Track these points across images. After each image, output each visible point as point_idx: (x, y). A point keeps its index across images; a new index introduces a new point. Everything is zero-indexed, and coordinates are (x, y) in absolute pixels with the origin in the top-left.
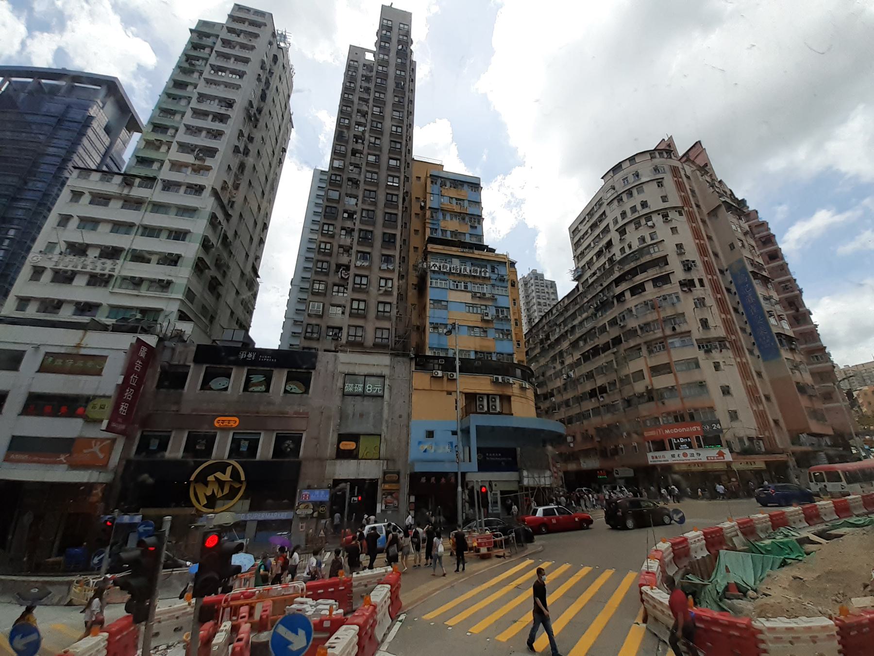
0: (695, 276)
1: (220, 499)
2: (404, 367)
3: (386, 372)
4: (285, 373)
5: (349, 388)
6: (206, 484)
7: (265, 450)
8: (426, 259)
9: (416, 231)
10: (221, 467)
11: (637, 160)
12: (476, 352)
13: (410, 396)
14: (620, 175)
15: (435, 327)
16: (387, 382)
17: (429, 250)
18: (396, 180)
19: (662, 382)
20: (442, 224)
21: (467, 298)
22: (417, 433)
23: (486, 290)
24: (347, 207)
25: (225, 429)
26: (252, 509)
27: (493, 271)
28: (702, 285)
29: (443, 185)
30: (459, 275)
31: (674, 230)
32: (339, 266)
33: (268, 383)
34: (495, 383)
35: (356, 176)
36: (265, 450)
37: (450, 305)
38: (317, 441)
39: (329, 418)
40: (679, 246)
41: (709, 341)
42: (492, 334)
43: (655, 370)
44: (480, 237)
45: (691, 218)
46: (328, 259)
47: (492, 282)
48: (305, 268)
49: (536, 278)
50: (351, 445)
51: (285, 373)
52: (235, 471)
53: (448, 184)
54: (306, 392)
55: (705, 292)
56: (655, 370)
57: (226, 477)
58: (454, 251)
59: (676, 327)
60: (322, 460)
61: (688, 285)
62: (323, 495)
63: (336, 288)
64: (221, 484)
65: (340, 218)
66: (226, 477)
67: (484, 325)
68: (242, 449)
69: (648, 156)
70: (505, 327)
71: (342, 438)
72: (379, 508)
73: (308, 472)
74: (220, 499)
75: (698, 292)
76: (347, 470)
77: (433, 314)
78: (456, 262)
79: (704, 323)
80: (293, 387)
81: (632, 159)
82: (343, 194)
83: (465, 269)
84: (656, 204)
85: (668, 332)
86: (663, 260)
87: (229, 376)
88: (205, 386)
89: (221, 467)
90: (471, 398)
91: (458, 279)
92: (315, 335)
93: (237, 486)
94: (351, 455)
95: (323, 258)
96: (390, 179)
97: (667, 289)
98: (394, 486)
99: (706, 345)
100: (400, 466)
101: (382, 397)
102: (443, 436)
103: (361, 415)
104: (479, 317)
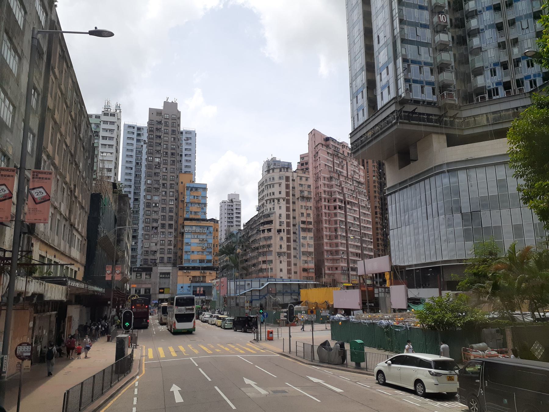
0: (282, 228)
2: (176, 269)
3: (170, 271)
4: (145, 273)
5: (161, 276)
7: (142, 292)
10: (134, 296)
11: (275, 171)
14: (269, 175)
15: (186, 252)
17: (185, 224)
19: (264, 266)
20: (190, 209)
21: (197, 241)
22: (179, 287)
23: (204, 237)
28: (284, 232)
29: (192, 190)
31: (280, 207)
32: (153, 227)
33: (141, 275)
35: (156, 186)
36: (142, 292)
37: (192, 244)
40: (280, 215)
41: (281, 253)
42: (205, 253)
43: (264, 262)
44: (205, 213)
45: (288, 202)
46: (148, 225)
49: (275, 164)
50: (162, 291)
51: (145, 273)
53: (193, 189)
55: (284, 235)
56: (264, 262)
58: (194, 223)
60: (156, 294)
61: (279, 231)
69: (279, 170)
70: (210, 250)
71: (160, 289)
73: (153, 296)
75: (282, 234)
76: (161, 296)
77: (186, 248)
78: (194, 228)
79: (281, 246)
80: (147, 277)
84: (277, 195)
86: (271, 222)
94: (163, 293)
97: (270, 234)
99: (280, 254)
102: (186, 288)
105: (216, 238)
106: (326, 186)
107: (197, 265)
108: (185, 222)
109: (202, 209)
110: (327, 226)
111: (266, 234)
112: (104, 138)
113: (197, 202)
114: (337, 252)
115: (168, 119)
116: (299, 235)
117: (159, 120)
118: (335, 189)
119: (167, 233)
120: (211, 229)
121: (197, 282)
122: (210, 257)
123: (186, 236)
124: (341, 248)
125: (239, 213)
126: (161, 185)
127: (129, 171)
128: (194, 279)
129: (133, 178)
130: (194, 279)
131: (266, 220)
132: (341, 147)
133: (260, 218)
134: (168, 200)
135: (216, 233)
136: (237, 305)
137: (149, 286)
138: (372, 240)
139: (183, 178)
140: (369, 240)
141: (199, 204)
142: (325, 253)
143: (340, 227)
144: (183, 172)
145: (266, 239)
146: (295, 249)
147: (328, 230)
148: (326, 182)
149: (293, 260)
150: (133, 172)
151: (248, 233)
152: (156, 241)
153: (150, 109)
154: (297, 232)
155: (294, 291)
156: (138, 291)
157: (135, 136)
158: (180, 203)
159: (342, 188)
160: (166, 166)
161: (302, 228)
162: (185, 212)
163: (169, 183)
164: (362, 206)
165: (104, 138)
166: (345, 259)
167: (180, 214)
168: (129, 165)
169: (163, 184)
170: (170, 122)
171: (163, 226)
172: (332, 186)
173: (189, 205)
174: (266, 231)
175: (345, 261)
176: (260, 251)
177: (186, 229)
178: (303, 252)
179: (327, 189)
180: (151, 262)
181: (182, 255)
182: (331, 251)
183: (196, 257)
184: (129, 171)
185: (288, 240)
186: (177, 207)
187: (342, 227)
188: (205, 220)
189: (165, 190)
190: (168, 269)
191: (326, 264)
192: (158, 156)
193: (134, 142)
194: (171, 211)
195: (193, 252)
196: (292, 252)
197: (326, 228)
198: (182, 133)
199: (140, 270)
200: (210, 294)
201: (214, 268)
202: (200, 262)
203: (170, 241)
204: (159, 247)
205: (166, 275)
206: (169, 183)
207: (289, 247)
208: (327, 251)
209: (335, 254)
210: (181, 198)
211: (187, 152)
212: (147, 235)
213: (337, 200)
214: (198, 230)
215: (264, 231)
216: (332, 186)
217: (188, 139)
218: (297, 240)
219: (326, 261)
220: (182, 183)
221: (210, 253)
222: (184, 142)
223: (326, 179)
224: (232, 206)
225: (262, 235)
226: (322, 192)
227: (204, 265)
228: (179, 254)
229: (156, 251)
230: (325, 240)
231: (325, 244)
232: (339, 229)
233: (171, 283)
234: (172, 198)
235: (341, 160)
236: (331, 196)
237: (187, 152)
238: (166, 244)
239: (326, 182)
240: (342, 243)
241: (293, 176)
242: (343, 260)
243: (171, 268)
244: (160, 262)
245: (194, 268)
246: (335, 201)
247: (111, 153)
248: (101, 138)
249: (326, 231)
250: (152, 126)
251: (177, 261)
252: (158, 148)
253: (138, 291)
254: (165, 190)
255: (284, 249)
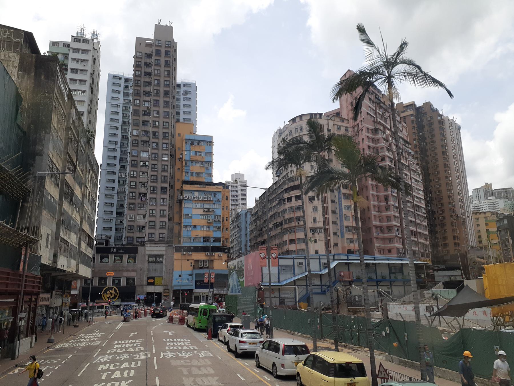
1: (112, 298)
3: (164, 253)
4: (127, 255)
5: (151, 260)
6: (107, 294)
7: (123, 283)
8: (182, 194)
9: (179, 169)
10: (111, 288)
11: (303, 118)
12: (204, 238)
13: (173, 262)
14: (295, 125)
15: (186, 227)
16: (164, 257)
17: (184, 188)
18: (167, 156)
19: (292, 247)
20: (191, 169)
22: (176, 275)
24: (142, 159)
25: (110, 276)
26: (122, 301)
27: (215, 196)
28: (318, 200)
29: (192, 144)
30: (198, 200)
32: (140, 194)
33: (121, 259)
34: (207, 255)
35: (145, 138)
36: (123, 283)
37: (194, 217)
38: (141, 280)
39: (144, 271)
41: (315, 228)
42: (212, 229)
43: (292, 241)
44: (210, 175)
46: (134, 190)
47: (214, 202)
48: (109, 156)
50: (152, 281)
51: (127, 255)
52: (115, 289)
54: (135, 262)
56: (292, 241)
57: (113, 292)
58: (195, 187)
59: (299, 222)
62: (142, 297)
63: (140, 205)
64: (111, 294)
65: (139, 166)
66: (113, 292)
67: (208, 225)
68: (117, 282)
70: (219, 225)
71: (149, 278)
72: (162, 301)
73: (138, 290)
74: (112, 298)
76: (151, 289)
77: (185, 221)
78: (196, 194)
79: (315, 219)
80: (130, 261)
81: (301, 117)
82: (139, 151)
83: (200, 197)
85: (297, 224)
87: (108, 258)
88: (101, 262)
89: (111, 288)
90: (197, 261)
91: (197, 202)
92: (132, 231)
93: (116, 294)
94: (152, 284)
95: (132, 190)
96: (164, 156)
98: (167, 294)
99: (314, 230)
100: (169, 288)
101: (163, 262)
102: (185, 276)
103: (155, 270)
104: (206, 220)
105: (225, 208)
106: (371, 140)
107: (201, 244)
108: (184, 185)
109: (207, 169)
110: (375, 193)
111: (294, 203)
112: (74, 71)
113: (199, 159)
114: (389, 228)
115: (161, 46)
116: (340, 204)
117: (148, 52)
118: (383, 144)
119: (158, 200)
120: (220, 196)
121: (201, 268)
122: (218, 234)
123: (185, 205)
124: (394, 223)
125: (245, 195)
126: (151, 135)
127: (114, 132)
128: (197, 264)
129: (118, 139)
130: (197, 264)
131: (291, 184)
132: (381, 96)
133: (284, 182)
134: (160, 155)
135: (226, 202)
136: (282, 302)
137: (133, 274)
138: (425, 216)
139: (180, 129)
140: (423, 215)
141: (202, 162)
142: (374, 230)
143: (392, 195)
144: (181, 120)
145: (293, 209)
146: (334, 223)
147: (376, 198)
148: (371, 135)
149: (332, 239)
150: (119, 132)
151: (264, 208)
152: (144, 213)
153: (138, 39)
154: (337, 200)
155: (384, 278)
156: (117, 282)
157: (121, 89)
158: (177, 161)
159: (390, 144)
160: (157, 109)
161: (345, 195)
162: (184, 173)
163: (161, 131)
164: (412, 170)
165: (74, 71)
166: (400, 238)
167: (177, 176)
168: (114, 124)
169: (154, 133)
170: (163, 51)
171: (154, 190)
172: (378, 140)
173: (189, 164)
174: (293, 199)
175: (400, 242)
176: (285, 226)
177: (186, 195)
178: (346, 227)
179: (371, 144)
180: (137, 242)
181: (180, 233)
182: (381, 227)
183: (200, 233)
184: (114, 132)
185: (325, 211)
186: (173, 166)
187: (394, 194)
188: (212, 184)
189: (156, 141)
190: (160, 250)
191: (376, 245)
192: (147, 98)
193: (121, 96)
194: (164, 170)
195: (195, 227)
196: (331, 228)
197: (373, 195)
198: (179, 86)
199: (120, 251)
200: (225, 285)
201: (225, 249)
202: (204, 241)
203: (163, 210)
204: (148, 219)
205: (157, 259)
206: (161, 131)
207: (326, 221)
208: (376, 227)
209: (386, 230)
210: (178, 155)
211: (186, 109)
212: (132, 204)
213: (387, 159)
214: (202, 197)
215: (290, 199)
216: (378, 140)
217: (186, 93)
218: (338, 211)
219: (375, 240)
220: (179, 134)
221: (219, 228)
222: (182, 97)
223: (370, 131)
224: (237, 187)
225: (288, 205)
226: (366, 147)
227: (213, 244)
228: (176, 229)
229: (144, 227)
230: (373, 213)
231: (373, 217)
232: (391, 198)
233: (164, 269)
234: (166, 152)
235: (383, 111)
236: (377, 153)
237: (186, 109)
238: (158, 215)
239: (371, 135)
240: (395, 217)
241: (328, 125)
242: (398, 239)
243: (164, 248)
244: (149, 241)
245: (197, 249)
246: (383, 159)
247: (84, 92)
248: (69, 71)
249: (374, 201)
250: (140, 60)
251: (172, 241)
252: (148, 89)
253: (117, 282)
254: (156, 141)
255: (320, 223)
